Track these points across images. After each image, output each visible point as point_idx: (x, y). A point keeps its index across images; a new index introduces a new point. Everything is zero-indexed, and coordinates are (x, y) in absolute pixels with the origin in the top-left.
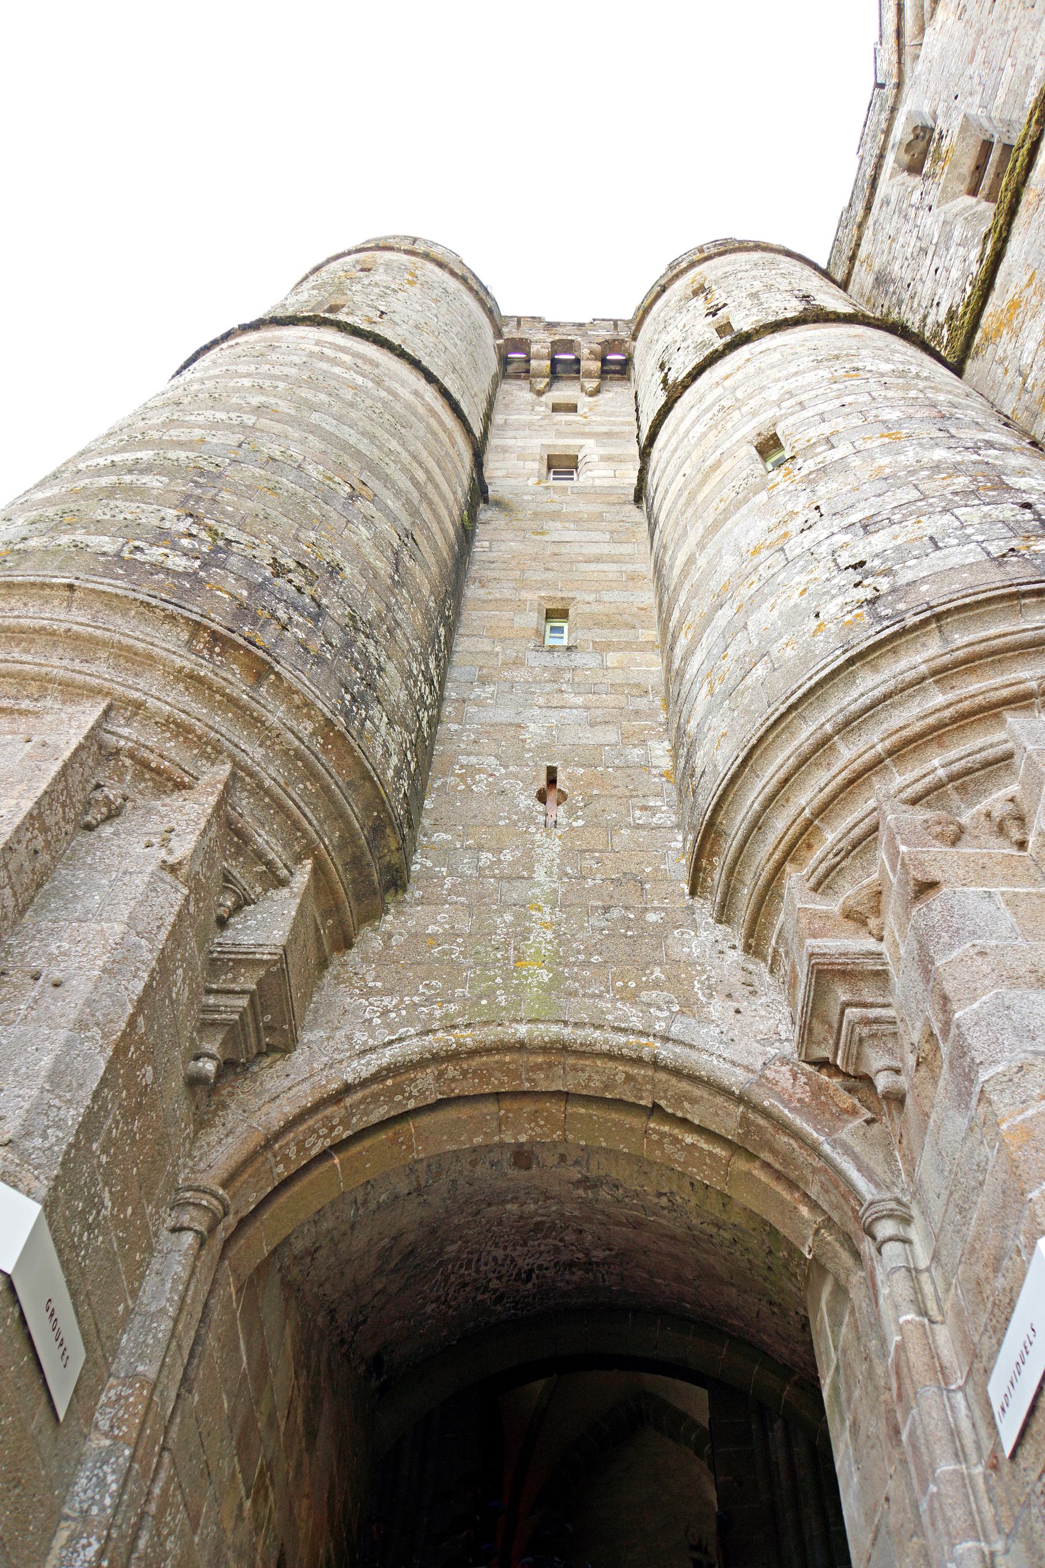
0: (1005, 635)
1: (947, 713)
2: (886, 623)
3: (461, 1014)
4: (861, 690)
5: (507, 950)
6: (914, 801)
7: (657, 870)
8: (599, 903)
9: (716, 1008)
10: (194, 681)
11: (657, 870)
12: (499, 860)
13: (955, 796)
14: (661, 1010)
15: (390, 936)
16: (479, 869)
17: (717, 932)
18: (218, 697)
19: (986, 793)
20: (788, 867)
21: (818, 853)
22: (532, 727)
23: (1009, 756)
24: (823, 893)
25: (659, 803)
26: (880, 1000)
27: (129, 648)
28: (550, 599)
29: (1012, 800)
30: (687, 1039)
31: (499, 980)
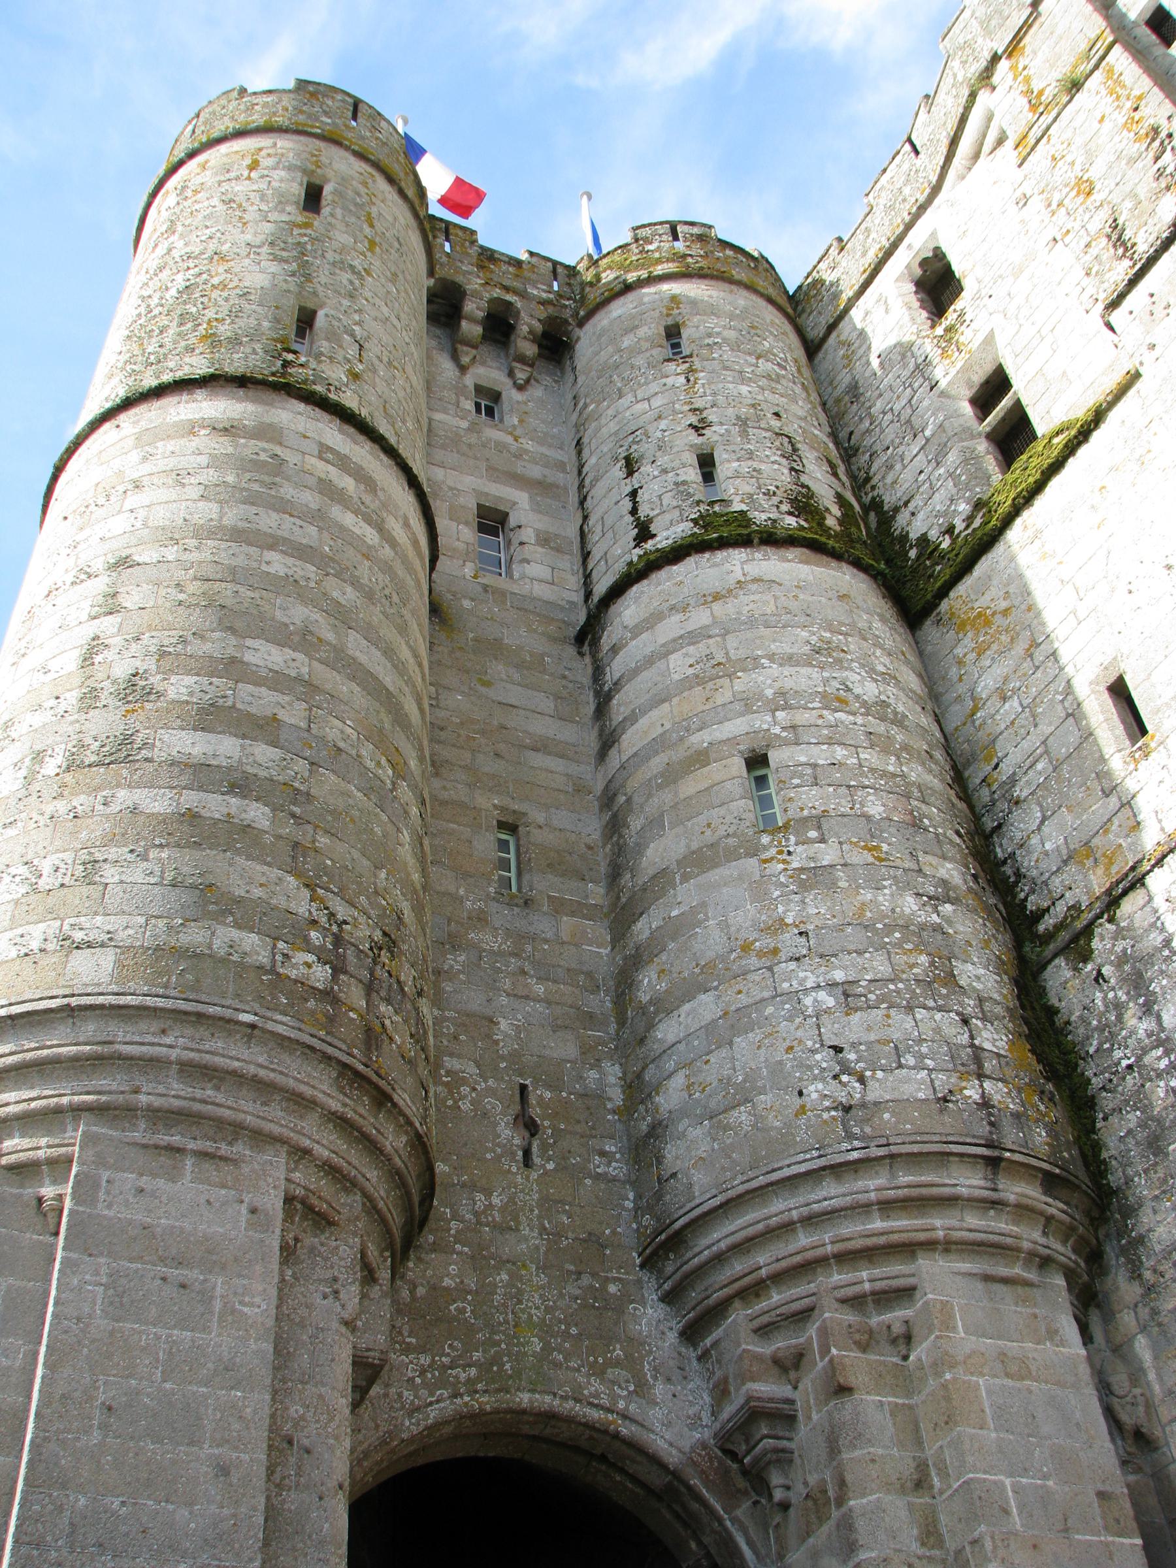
0: (932, 1185)
1: (882, 1240)
2: (856, 1143)
3: (478, 1379)
4: (824, 1193)
5: (507, 1314)
6: (844, 1301)
7: (614, 1232)
8: (572, 1268)
9: (660, 1390)
10: (341, 1123)
11: (614, 1232)
12: (491, 1204)
13: (871, 1305)
14: (622, 1389)
15: (415, 1287)
16: (476, 1214)
17: (659, 1311)
18: (356, 1134)
19: (892, 1309)
20: (737, 1304)
21: (764, 1305)
22: (504, 1024)
23: (913, 1289)
24: (760, 1336)
25: (613, 1149)
26: (787, 1434)
27: (300, 1096)
28: (503, 809)
29: (907, 1322)
30: (640, 1419)
31: (503, 1346)
